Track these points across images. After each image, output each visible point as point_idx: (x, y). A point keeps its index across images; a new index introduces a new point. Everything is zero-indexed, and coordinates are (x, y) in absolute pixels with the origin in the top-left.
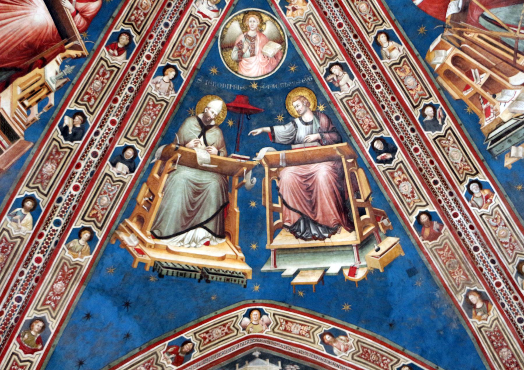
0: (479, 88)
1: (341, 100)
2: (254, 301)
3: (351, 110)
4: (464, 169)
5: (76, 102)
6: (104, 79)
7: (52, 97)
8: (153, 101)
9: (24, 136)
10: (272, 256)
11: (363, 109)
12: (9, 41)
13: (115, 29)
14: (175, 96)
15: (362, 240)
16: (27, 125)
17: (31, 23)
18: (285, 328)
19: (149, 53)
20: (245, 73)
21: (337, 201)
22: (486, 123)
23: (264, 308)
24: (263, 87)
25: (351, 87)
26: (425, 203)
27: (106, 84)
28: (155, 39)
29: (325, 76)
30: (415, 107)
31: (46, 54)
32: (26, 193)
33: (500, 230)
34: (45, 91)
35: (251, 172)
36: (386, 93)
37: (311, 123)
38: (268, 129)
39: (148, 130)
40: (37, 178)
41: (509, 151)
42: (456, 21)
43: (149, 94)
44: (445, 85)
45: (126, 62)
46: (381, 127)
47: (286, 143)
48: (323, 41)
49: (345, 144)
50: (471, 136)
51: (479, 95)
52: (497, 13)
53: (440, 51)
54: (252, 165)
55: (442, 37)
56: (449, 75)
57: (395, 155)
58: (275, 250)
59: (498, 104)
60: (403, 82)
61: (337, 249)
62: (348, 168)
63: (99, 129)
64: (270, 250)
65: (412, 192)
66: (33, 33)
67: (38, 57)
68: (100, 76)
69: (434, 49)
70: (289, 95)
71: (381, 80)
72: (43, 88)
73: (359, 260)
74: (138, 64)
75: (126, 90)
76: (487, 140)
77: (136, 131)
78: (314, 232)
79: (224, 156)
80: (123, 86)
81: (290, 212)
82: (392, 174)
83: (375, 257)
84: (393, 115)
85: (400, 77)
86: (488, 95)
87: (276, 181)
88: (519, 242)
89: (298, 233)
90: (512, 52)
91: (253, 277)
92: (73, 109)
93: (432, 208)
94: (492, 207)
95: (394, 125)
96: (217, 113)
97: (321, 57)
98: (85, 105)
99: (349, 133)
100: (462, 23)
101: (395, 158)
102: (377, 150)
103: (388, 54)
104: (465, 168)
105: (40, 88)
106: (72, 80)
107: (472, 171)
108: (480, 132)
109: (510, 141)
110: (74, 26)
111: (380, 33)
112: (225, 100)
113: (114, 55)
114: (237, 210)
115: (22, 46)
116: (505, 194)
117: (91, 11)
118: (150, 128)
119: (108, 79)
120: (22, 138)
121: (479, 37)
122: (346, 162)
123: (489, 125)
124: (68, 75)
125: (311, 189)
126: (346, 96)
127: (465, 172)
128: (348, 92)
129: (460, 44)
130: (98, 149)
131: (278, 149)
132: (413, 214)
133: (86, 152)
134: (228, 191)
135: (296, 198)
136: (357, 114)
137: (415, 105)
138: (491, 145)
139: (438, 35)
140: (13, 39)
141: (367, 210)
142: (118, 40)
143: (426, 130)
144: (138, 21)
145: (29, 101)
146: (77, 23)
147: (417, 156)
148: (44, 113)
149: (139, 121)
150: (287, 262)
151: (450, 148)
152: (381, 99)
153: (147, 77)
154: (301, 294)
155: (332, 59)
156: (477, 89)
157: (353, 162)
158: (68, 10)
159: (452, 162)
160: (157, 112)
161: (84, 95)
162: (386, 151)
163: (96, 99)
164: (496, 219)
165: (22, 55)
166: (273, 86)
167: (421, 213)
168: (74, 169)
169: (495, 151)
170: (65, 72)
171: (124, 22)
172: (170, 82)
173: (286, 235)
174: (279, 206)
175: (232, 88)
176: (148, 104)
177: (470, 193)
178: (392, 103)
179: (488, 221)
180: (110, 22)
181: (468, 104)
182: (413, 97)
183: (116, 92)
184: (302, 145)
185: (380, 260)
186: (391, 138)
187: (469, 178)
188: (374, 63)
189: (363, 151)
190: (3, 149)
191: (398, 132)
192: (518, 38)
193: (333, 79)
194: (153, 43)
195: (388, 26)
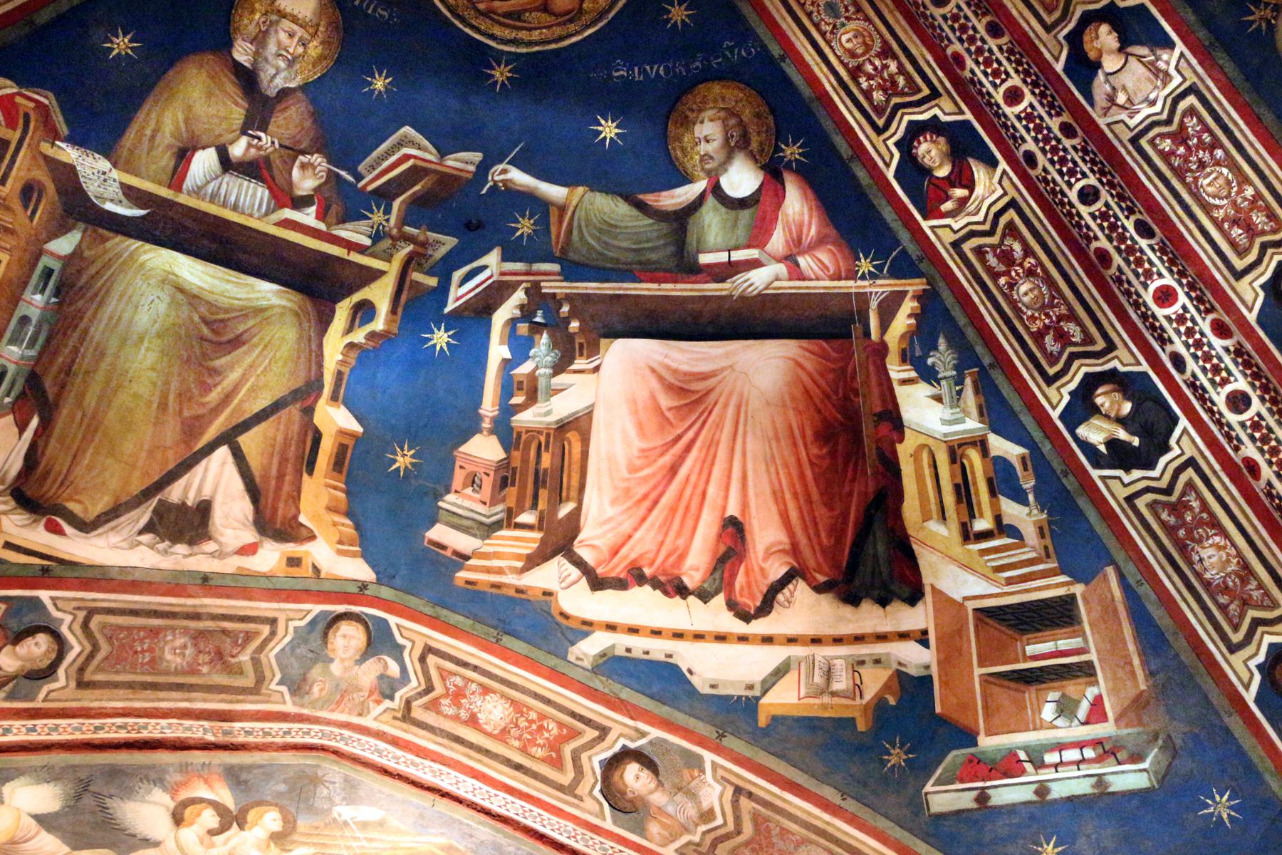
5: (1050, 380)
6: (1021, 265)
7: (1001, 446)
8: (1163, 136)
9: (1077, 578)
12: (792, 485)
13: (888, 165)
14: (1182, 55)
16: (1048, 556)
17: (768, 403)
19: (1002, 90)
27: (1041, 264)
28: (968, 50)
31: (871, 404)
32: (1252, 664)
34: (974, 455)
39: (1249, 192)
40: (1223, 608)
43: (1134, 141)
45: (1004, 172)
63: (1169, 348)
66: (798, 412)
67: (867, 428)
68: (1007, 273)
72: (962, 456)
74: (1022, 138)
75: (1084, 210)
77: (1236, 232)
80: (1070, 214)
92: (1066, 399)
98: (1073, 357)
105: (957, 467)
106: (978, 363)
110: (825, 285)
113: (963, 202)
115: (818, 457)
117: (806, 218)
118: (1247, 181)
119: (1028, 251)
120: (1078, 589)
124: (956, 368)
130: (1225, 382)
133: (1219, 423)
140: (789, 474)
142: (926, 172)
144: (894, 83)
145: (981, 516)
146: (821, 273)
148: (1036, 489)
149: (1207, 208)
153: (1081, 125)
158: (777, 284)
160: (1207, 138)
161: (1042, 347)
163: (1072, 317)
165: (845, 471)
168: (1259, 486)
170: (946, 372)
171: (879, 131)
172: (1128, 55)
176: (1166, 156)
180: (861, 173)
183: (1083, 243)
190: (1083, 658)
194: (977, 63)
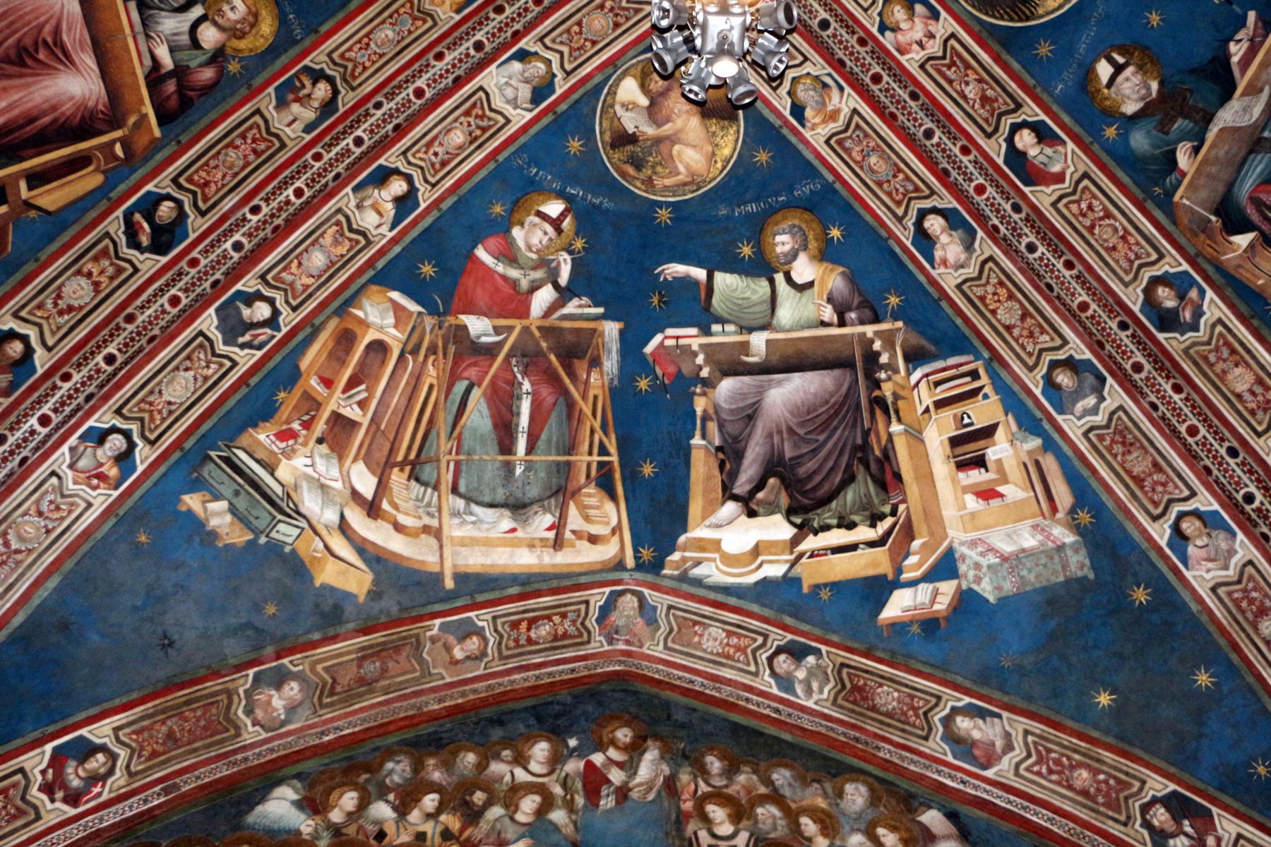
0: (331, 406)
1: (258, 112)
4: (151, 411)
11: (241, 163)
21: (11, 131)
22: (264, 436)
25: (287, 129)
26: (50, 342)
30: (263, 277)
33: (32, 523)
37: (195, 44)
41: (217, 497)
42: (455, 336)
44: (324, 336)
48: (381, 56)
49: (157, 133)
50: (228, 412)
51: (318, 410)
52: (480, 411)
53: (391, 314)
55: (420, 313)
56: (346, 339)
57: (151, 252)
59: (307, 451)
60: (313, 244)
62: (100, 147)
65: (70, 309)
69: (391, 300)
76: (229, 447)
82: (104, 253)
85: (322, 235)
86: (320, 427)
88: (20, 570)
90: (412, 456)
93: (42, 361)
94: (81, 493)
97: (347, 55)
99: (184, 139)
100: (452, 349)
101: (142, 253)
102: (156, 210)
103: (367, 203)
104: (155, 413)
107: (151, 431)
108: (242, 429)
109: (237, 493)
111: (409, 179)
116: (121, 512)
121: (431, 387)
122: (113, 142)
123: (260, 443)
125: (29, 62)
126: (266, 121)
127: (146, 416)
128: (277, 125)
129: (411, 353)
136: (231, 152)
137: (269, 277)
138: (219, 457)
139: (423, 306)
143: (217, 310)
147: (162, 306)
151: (192, 373)
152: (274, 204)
155: (344, 80)
156: (328, 403)
157: (116, 158)
159: (160, 383)
162: (157, 230)
164: (58, 508)
167: (24, 339)
169: (208, 470)
177: (100, 437)
179: (47, 492)
181: (294, 391)
182: (284, 269)
184: (138, 27)
186: (187, 236)
187: (134, 427)
192: (438, 460)
193: (303, 86)
195: (425, 196)
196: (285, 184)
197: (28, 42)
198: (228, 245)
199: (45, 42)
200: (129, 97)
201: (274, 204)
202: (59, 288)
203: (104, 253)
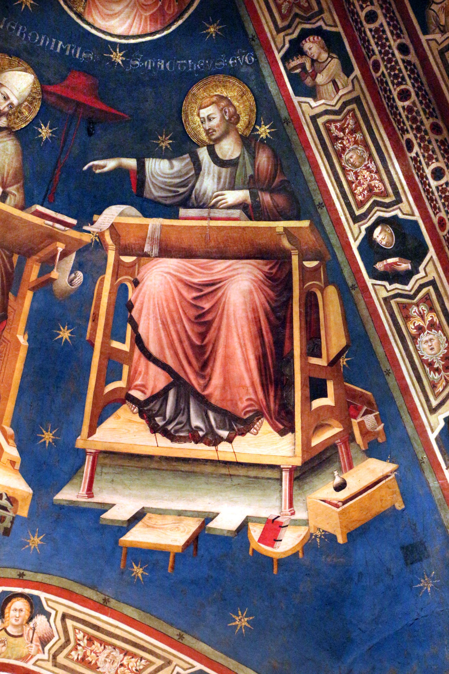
1: (314, 118)
2: (22, 575)
3: (333, 145)
10: (87, 468)
11: (361, 148)
15: (307, 458)
18: (85, 656)
20: (101, 23)
23: (43, 595)
24: (137, 63)
25: (341, 93)
29: (285, 59)
35: (73, 256)
36: (422, 113)
38: (131, 163)
46: (396, 193)
47: (168, 202)
49: (305, 223)
54: (80, 241)
58: (98, 454)
61: (242, 472)
62: (302, 281)
64: (83, 452)
70: (194, 90)
71: (416, 80)
73: (291, 505)
78: (196, 422)
79: (16, 206)
81: (147, 367)
82: (404, 308)
83: (330, 503)
84: (428, 165)
87: (130, 286)
89: (157, 419)
91: (30, 513)
95: (428, 192)
96: (15, 102)
99: (318, 199)
102: (378, 246)
112: (40, 77)
114: (23, 340)
122: (302, 267)
125: (209, 318)
126: (326, 112)
131: (146, 214)
132: (440, 411)
134: (9, 290)
135: (169, 335)
136: (345, 157)
141: (330, 387)
150: (120, 487)
152: (408, 124)
154: (138, 571)
155: (308, 20)
157: (316, 269)
166: (161, 64)
173: (130, 421)
174: (126, 347)
175: (63, 50)
178: (432, 136)
184: (204, 212)
185: (341, 513)
186: (416, 223)
188: (407, 41)
189: (346, 246)
191: (434, 208)
193: (303, 66)
196: (394, 107)
197: (192, 313)
198: (433, 183)
199: (195, 299)
200: (262, 241)
201: (408, 124)
202: (423, 361)
203: (404, 308)
